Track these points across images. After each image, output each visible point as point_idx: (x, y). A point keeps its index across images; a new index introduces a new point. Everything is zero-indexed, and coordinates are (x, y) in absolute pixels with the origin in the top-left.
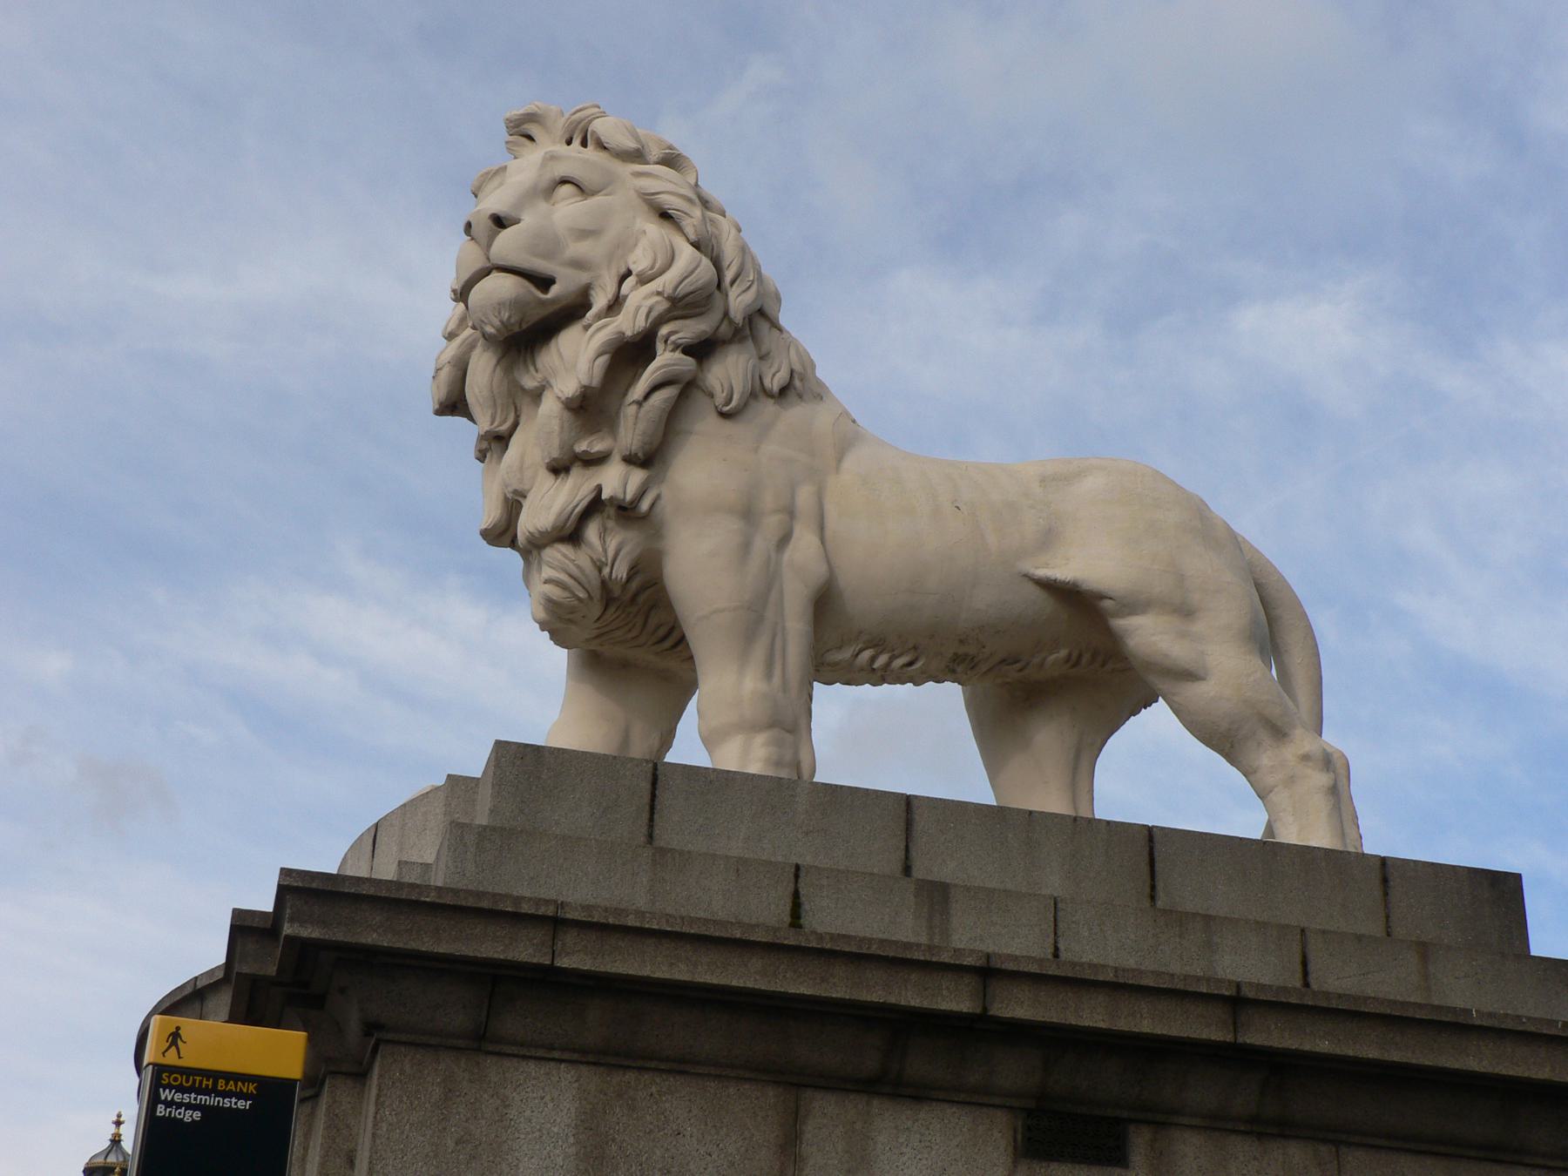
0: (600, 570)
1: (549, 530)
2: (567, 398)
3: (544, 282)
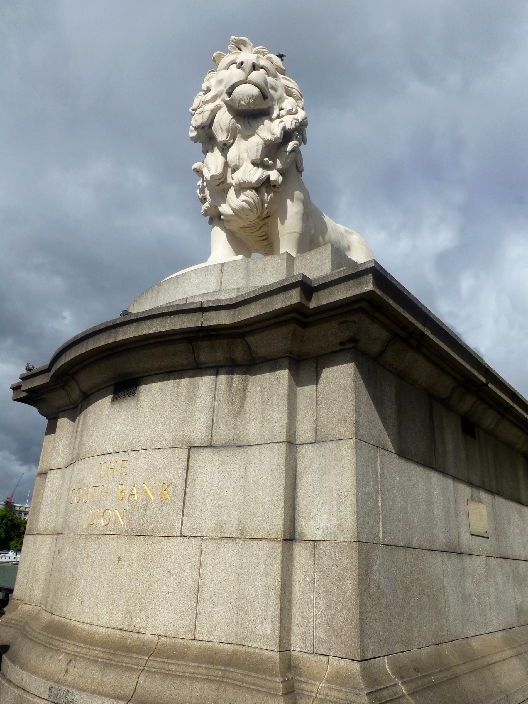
1: (253, 183)
2: (268, 140)
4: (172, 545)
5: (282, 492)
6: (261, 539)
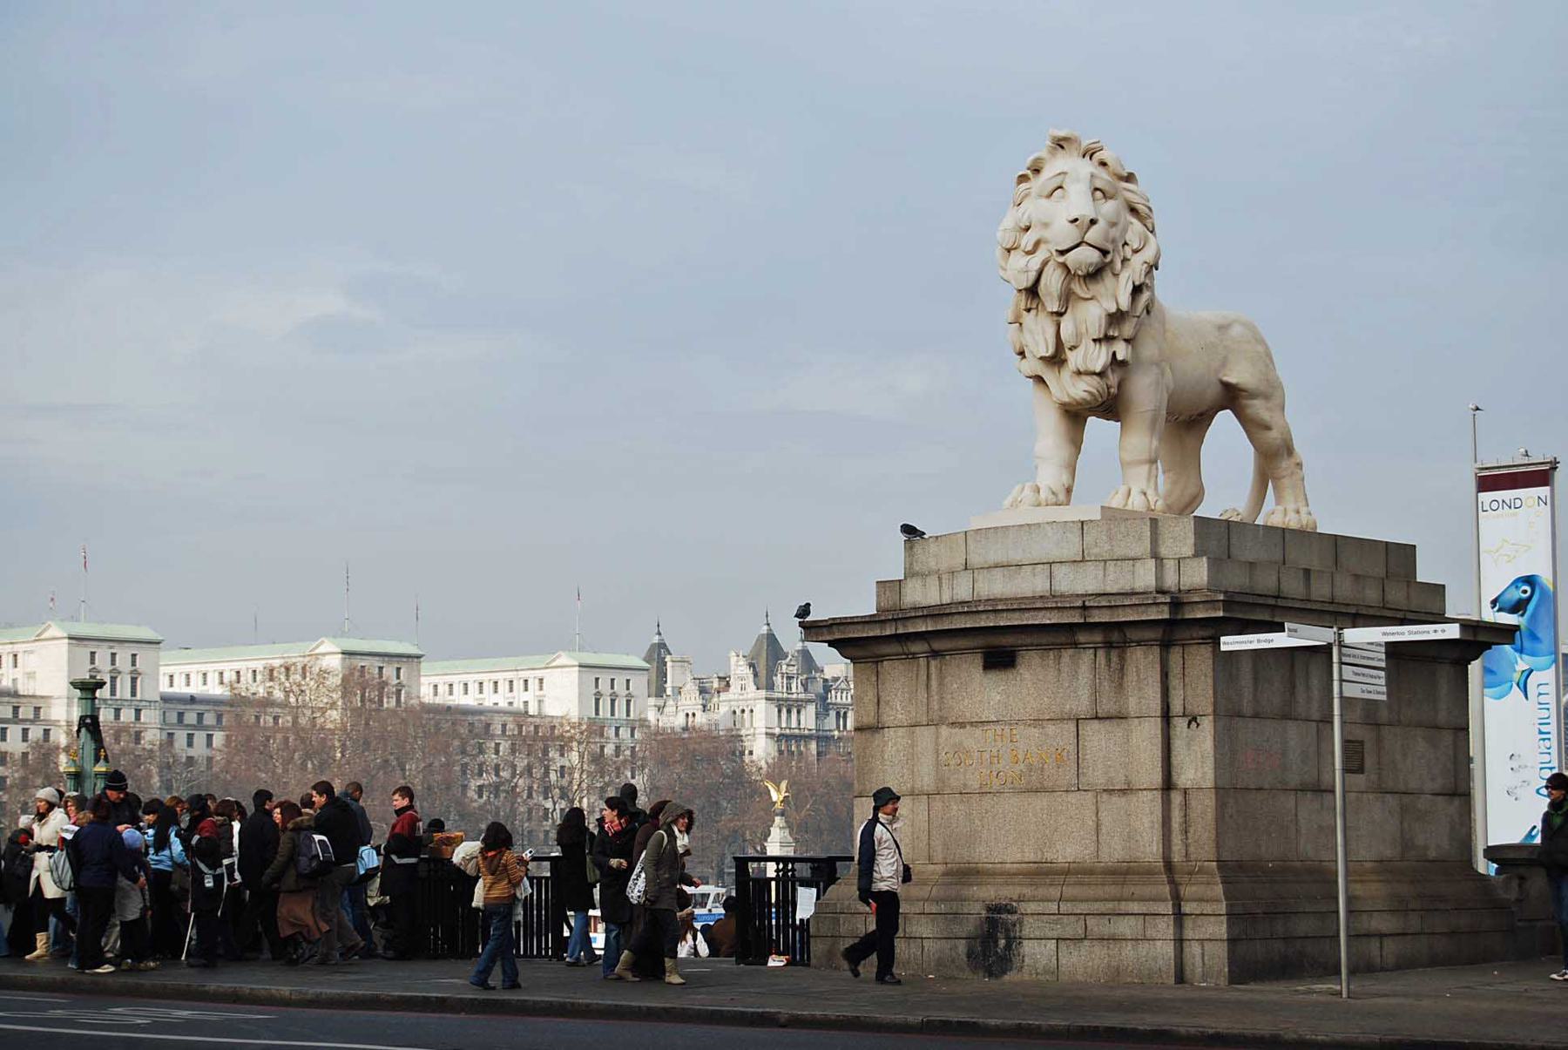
0: (1108, 389)
3: (1105, 253)
4: (1072, 798)
5: (1160, 755)
6: (1145, 789)
